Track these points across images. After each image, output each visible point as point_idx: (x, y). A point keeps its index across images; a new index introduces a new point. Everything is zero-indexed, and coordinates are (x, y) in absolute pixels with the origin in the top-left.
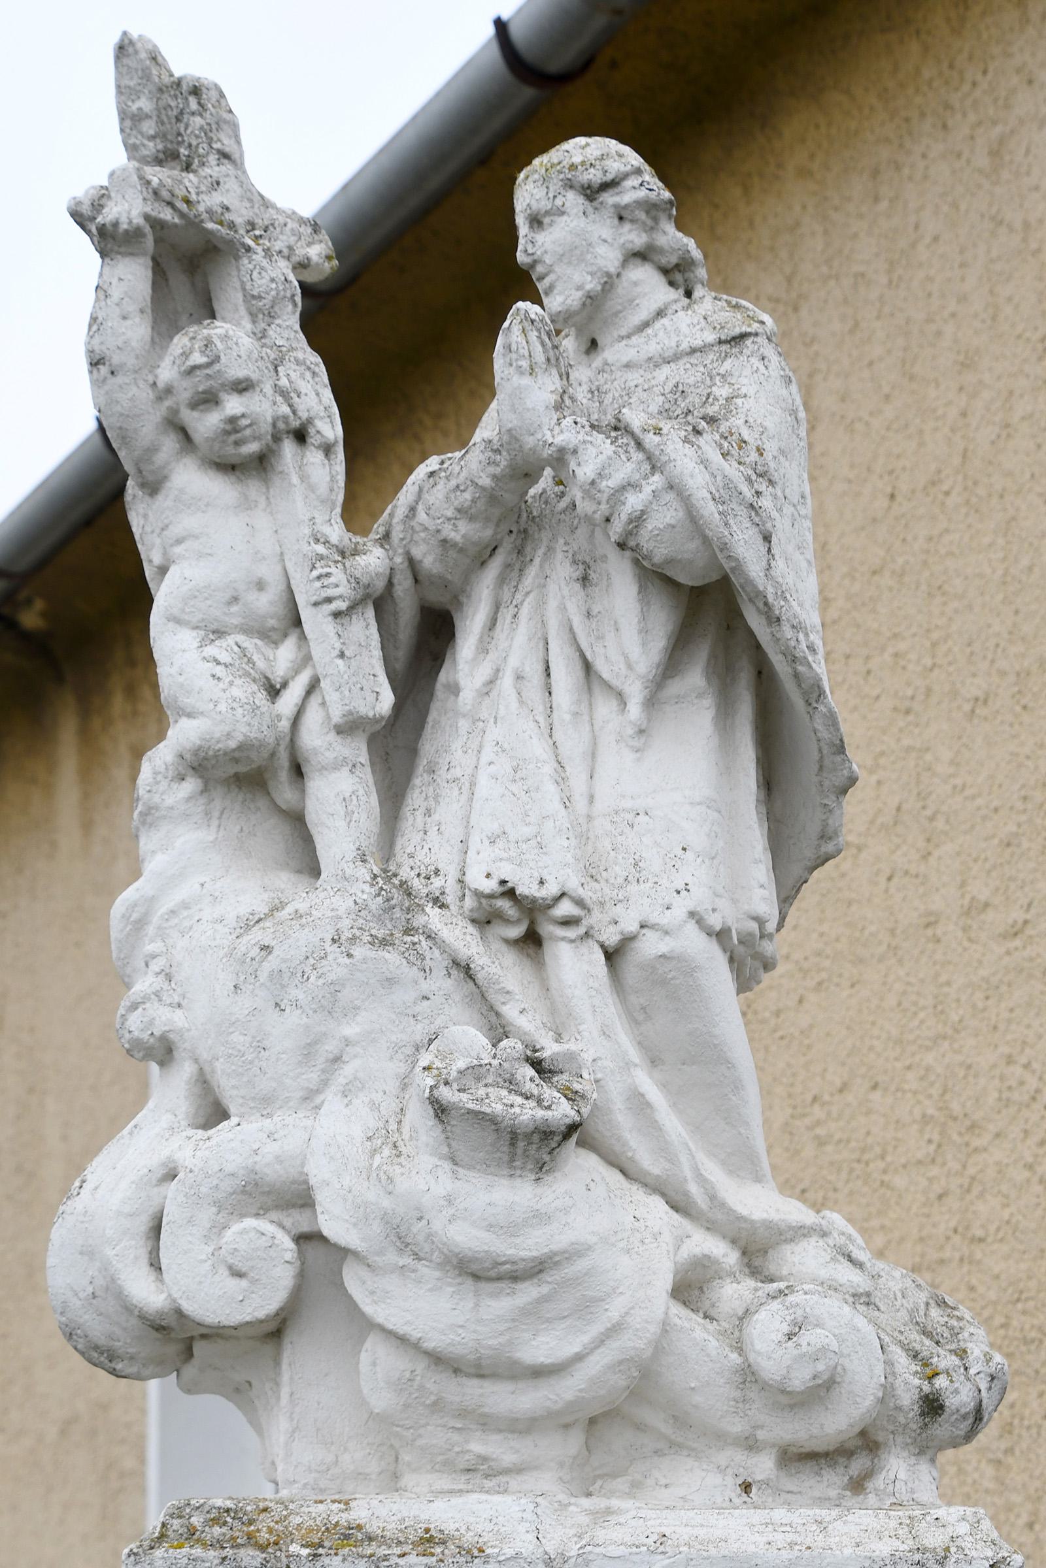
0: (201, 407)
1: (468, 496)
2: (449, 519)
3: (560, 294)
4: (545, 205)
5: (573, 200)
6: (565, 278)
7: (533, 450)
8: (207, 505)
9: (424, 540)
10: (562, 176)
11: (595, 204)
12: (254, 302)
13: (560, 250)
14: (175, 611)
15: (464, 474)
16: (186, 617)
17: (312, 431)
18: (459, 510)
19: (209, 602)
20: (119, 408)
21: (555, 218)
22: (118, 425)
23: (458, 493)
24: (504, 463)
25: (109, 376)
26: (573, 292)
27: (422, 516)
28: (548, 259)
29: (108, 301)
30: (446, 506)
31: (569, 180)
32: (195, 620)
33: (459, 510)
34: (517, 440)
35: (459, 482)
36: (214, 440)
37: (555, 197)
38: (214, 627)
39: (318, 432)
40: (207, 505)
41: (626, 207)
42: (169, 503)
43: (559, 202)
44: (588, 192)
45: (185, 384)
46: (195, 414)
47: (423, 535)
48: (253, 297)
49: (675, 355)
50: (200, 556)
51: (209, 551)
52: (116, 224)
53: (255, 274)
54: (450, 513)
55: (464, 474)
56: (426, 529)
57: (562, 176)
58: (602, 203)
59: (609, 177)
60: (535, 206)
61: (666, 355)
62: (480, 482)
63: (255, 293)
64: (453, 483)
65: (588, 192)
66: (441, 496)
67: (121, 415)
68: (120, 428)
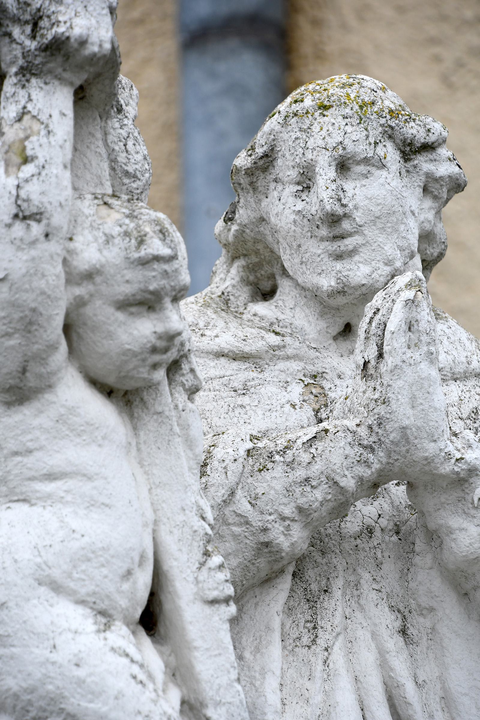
0: (133, 309)
1: (318, 495)
2: (284, 519)
3: (366, 262)
4: (362, 149)
5: (390, 152)
6: (375, 246)
7: (428, 461)
8: (104, 438)
9: (235, 537)
10: (383, 121)
11: (409, 165)
12: (126, 181)
13: (376, 210)
14: (56, 574)
15: (317, 467)
16: (72, 585)
17: (185, 367)
18: (300, 510)
19: (105, 571)
20: (42, 284)
21: (373, 170)
22: (33, 305)
23: (308, 489)
24: (376, 466)
25: (42, 238)
26: (381, 265)
27: (243, 505)
28: (359, 217)
29: (52, 139)
30: (285, 500)
31: (392, 128)
32: (83, 591)
33: (300, 510)
34: (408, 441)
35: (310, 473)
36: (135, 354)
37: (376, 143)
38: (102, 606)
39: (192, 371)
40: (104, 438)
41: (437, 180)
42: (44, 421)
43: (380, 151)
44: (408, 149)
45: (129, 275)
46: (120, 316)
47: (236, 529)
48: (127, 174)
49: (465, 372)
50: (92, 504)
51: (107, 501)
52: (83, 42)
53: (130, 143)
54: (288, 511)
55: (317, 467)
56: (247, 523)
57: (383, 121)
58: (415, 167)
59: (432, 138)
60: (350, 147)
61: (457, 370)
62: (343, 482)
63: (130, 169)
64: (300, 473)
65: (408, 149)
66: (278, 485)
67: (43, 293)
68: (34, 310)
